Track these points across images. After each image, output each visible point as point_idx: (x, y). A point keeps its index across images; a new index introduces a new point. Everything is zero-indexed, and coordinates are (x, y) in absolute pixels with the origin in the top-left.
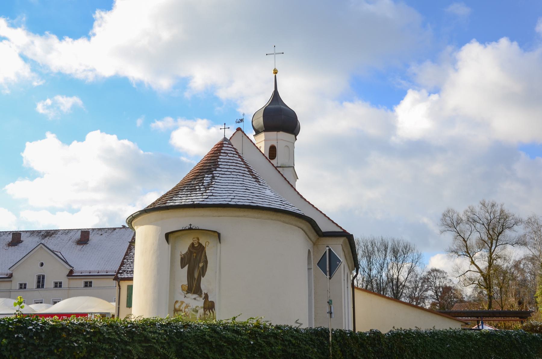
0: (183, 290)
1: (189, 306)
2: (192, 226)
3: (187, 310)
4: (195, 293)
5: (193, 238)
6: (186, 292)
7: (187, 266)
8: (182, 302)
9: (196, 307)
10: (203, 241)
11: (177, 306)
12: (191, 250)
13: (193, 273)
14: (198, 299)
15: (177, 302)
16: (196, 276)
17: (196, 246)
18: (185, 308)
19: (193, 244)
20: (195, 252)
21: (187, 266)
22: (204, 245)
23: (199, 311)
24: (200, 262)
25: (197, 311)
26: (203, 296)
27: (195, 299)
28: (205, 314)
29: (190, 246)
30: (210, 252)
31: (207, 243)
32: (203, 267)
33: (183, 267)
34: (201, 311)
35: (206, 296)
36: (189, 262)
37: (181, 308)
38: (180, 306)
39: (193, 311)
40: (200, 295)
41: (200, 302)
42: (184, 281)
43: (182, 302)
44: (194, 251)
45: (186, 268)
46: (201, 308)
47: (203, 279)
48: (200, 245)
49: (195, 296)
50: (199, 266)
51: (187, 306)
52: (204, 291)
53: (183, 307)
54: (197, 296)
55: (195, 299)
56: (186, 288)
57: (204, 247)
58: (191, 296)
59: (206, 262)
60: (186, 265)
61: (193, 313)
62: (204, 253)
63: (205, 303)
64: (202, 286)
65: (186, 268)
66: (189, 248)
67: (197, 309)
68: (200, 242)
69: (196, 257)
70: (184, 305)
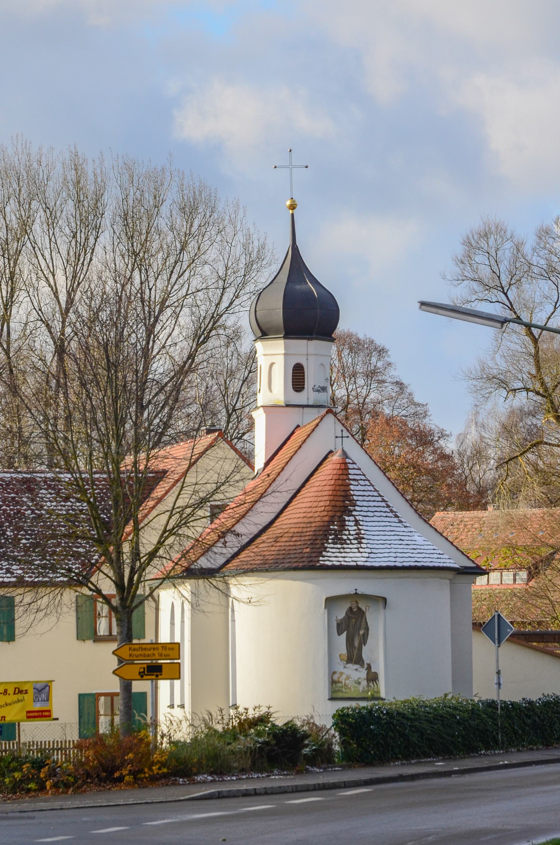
0: (341, 660)
1: (350, 677)
2: (357, 592)
3: (347, 682)
4: (356, 663)
5: (351, 602)
6: (345, 662)
7: (345, 632)
8: (342, 674)
9: (359, 679)
10: (362, 605)
11: (335, 677)
12: (350, 615)
13: (353, 641)
14: (360, 669)
15: (334, 673)
16: (356, 643)
17: (355, 610)
18: (345, 680)
19: (351, 609)
20: (354, 618)
21: (345, 632)
22: (364, 609)
23: (362, 683)
24: (359, 629)
25: (359, 683)
26: (366, 666)
27: (356, 670)
28: (368, 686)
29: (348, 610)
30: (370, 617)
31: (368, 608)
32: (364, 635)
33: (339, 634)
34: (364, 683)
35: (369, 667)
36: (347, 628)
37: (341, 680)
38: (339, 678)
39: (355, 683)
40: (362, 666)
41: (362, 674)
42: (343, 650)
43: (342, 674)
44: (353, 616)
45: (344, 635)
46: (364, 679)
47: (364, 648)
48: (359, 609)
49: (356, 666)
50: (359, 633)
51: (348, 678)
52: (366, 662)
53: (342, 679)
54: (359, 666)
55: (356, 670)
56: (346, 658)
57: (363, 612)
58: (352, 667)
59: (367, 629)
60: (344, 632)
61: (356, 685)
62: (364, 618)
63: (368, 674)
64: (364, 656)
65: (344, 635)
66: (346, 613)
67: (360, 680)
68: (360, 606)
69: (356, 622)
70: (344, 676)
